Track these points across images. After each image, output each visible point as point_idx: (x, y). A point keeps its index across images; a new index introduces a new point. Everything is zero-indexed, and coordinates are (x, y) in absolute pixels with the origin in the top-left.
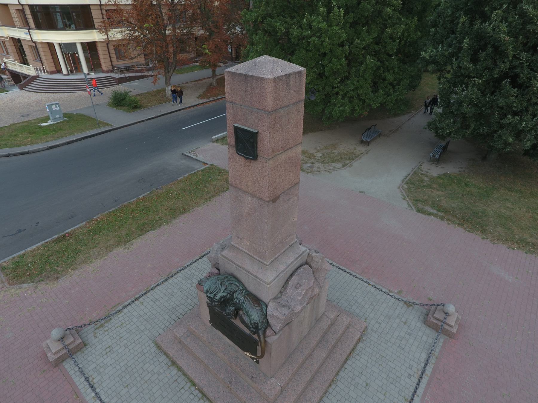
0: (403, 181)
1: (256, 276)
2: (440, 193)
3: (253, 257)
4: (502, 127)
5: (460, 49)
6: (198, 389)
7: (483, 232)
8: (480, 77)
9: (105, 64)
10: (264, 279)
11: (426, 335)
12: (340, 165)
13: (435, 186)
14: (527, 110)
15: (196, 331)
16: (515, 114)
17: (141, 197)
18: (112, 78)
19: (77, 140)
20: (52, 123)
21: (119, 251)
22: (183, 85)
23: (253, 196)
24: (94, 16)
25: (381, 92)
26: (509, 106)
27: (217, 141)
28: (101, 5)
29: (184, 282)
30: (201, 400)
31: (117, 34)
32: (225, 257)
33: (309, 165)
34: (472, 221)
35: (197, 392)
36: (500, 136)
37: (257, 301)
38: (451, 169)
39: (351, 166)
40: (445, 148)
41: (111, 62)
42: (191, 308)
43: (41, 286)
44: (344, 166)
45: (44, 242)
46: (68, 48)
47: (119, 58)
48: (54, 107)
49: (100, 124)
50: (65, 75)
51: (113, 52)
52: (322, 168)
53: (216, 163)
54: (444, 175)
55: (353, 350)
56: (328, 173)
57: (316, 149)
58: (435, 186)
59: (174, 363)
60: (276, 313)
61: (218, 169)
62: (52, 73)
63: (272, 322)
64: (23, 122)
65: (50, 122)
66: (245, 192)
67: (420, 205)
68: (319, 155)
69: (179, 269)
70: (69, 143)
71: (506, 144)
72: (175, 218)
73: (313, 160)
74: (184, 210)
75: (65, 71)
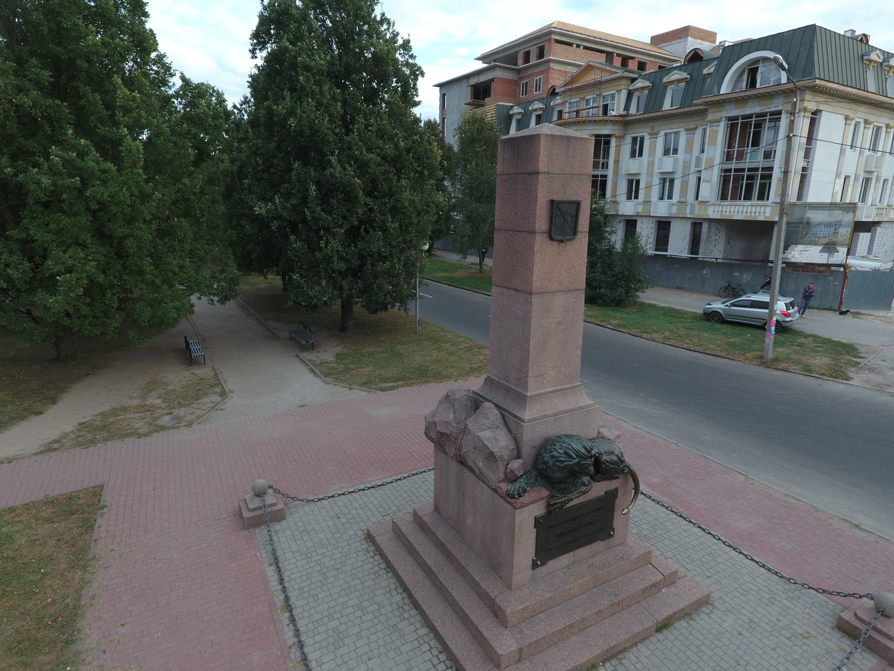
0: (318, 376)
1: (581, 408)
2: (366, 369)
3: (563, 390)
4: (376, 277)
5: (304, 200)
6: (604, 662)
7: (447, 377)
13: (352, 366)
14: (391, 255)
15: (528, 604)
23: (568, 291)
26: (380, 254)
29: (345, 650)
30: (623, 661)
32: (533, 420)
35: (608, 664)
36: (379, 287)
39: (232, 392)
42: (426, 647)
44: (223, 394)
52: (198, 412)
54: (338, 356)
56: (219, 412)
57: (131, 398)
58: (352, 366)
60: (616, 433)
66: (554, 292)
69: (295, 654)
72: (68, 642)
73: (159, 411)
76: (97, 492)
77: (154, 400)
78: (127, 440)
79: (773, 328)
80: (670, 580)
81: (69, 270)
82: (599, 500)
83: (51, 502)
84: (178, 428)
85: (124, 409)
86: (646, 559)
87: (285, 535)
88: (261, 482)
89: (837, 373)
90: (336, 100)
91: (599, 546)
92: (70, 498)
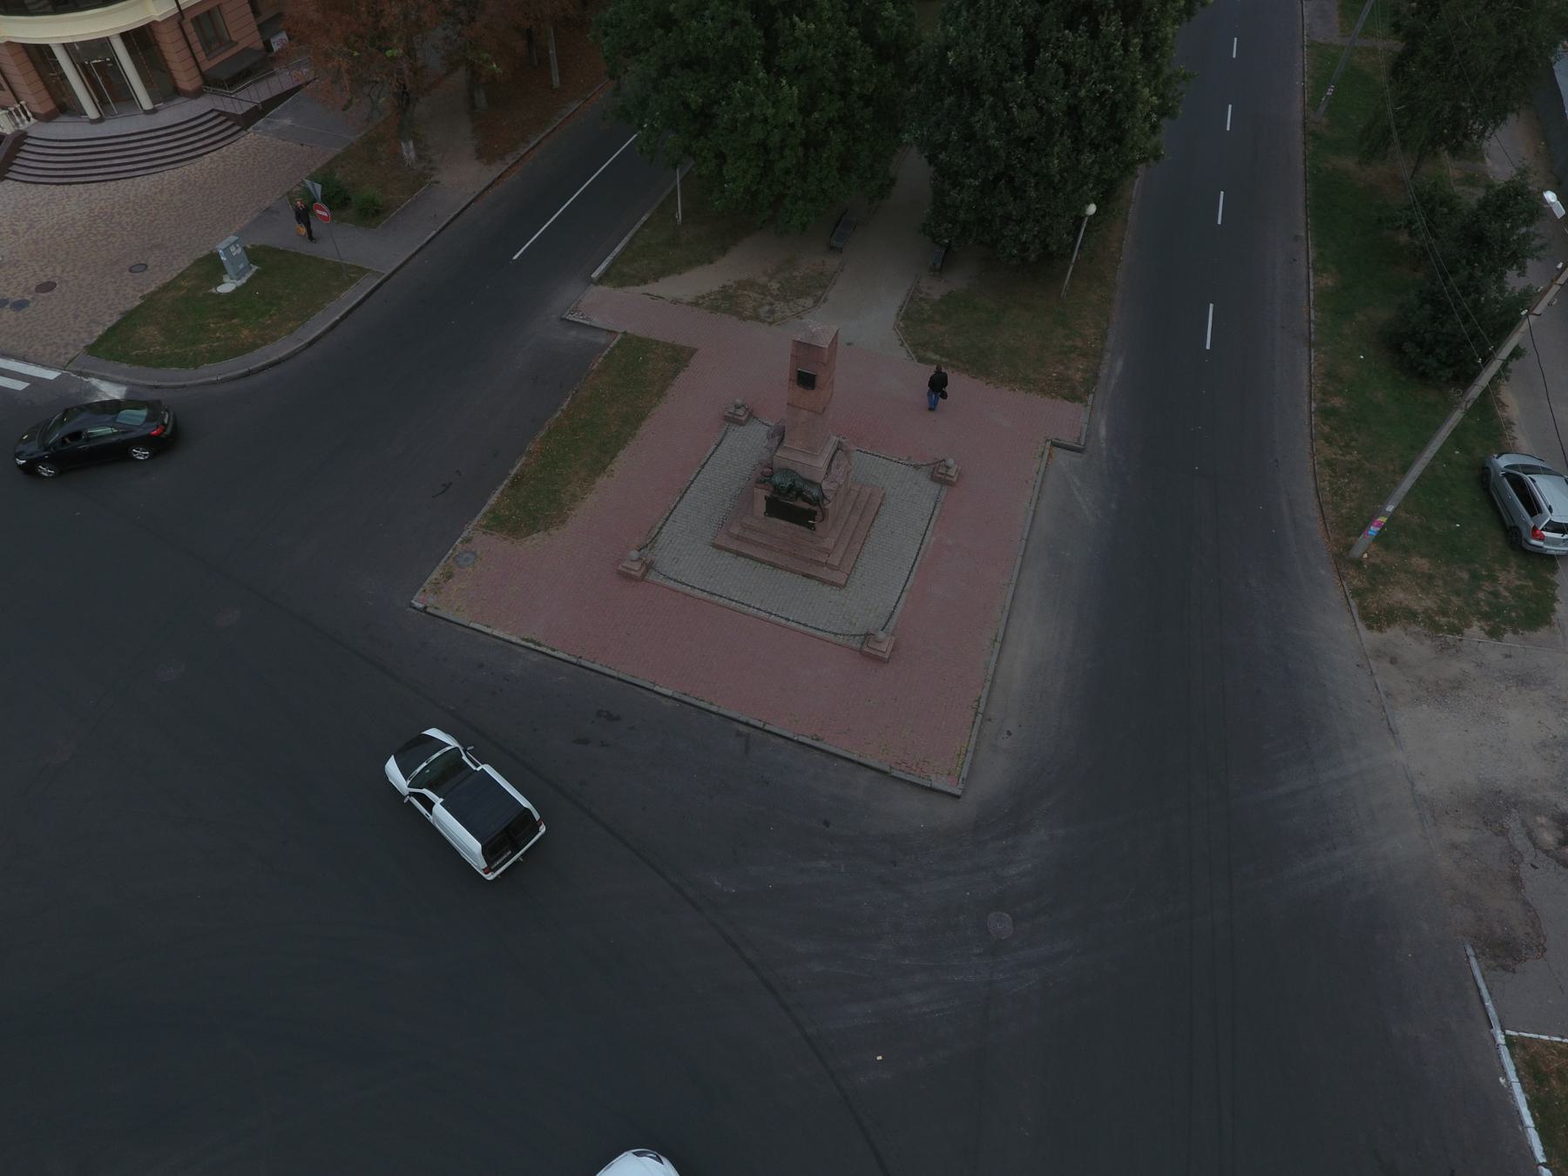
10: (814, 465)
11: (934, 488)
12: (809, 302)
18: (221, 113)
19: (342, 318)
20: (239, 283)
21: (602, 480)
27: (600, 281)
33: (767, 308)
37: (812, 483)
41: (197, 64)
43: (553, 531)
44: (816, 302)
45: (498, 493)
46: (91, 55)
47: (207, 45)
50: (93, 122)
51: (193, 37)
52: (788, 313)
59: (738, 554)
61: (639, 339)
62: (48, 118)
64: (165, 288)
68: (775, 285)
70: (333, 327)
76: (693, 352)
79: (1373, 530)
81: (734, 180)
82: (803, 510)
84: (763, 321)
85: (749, 284)
88: (739, 401)
92: (683, 349)
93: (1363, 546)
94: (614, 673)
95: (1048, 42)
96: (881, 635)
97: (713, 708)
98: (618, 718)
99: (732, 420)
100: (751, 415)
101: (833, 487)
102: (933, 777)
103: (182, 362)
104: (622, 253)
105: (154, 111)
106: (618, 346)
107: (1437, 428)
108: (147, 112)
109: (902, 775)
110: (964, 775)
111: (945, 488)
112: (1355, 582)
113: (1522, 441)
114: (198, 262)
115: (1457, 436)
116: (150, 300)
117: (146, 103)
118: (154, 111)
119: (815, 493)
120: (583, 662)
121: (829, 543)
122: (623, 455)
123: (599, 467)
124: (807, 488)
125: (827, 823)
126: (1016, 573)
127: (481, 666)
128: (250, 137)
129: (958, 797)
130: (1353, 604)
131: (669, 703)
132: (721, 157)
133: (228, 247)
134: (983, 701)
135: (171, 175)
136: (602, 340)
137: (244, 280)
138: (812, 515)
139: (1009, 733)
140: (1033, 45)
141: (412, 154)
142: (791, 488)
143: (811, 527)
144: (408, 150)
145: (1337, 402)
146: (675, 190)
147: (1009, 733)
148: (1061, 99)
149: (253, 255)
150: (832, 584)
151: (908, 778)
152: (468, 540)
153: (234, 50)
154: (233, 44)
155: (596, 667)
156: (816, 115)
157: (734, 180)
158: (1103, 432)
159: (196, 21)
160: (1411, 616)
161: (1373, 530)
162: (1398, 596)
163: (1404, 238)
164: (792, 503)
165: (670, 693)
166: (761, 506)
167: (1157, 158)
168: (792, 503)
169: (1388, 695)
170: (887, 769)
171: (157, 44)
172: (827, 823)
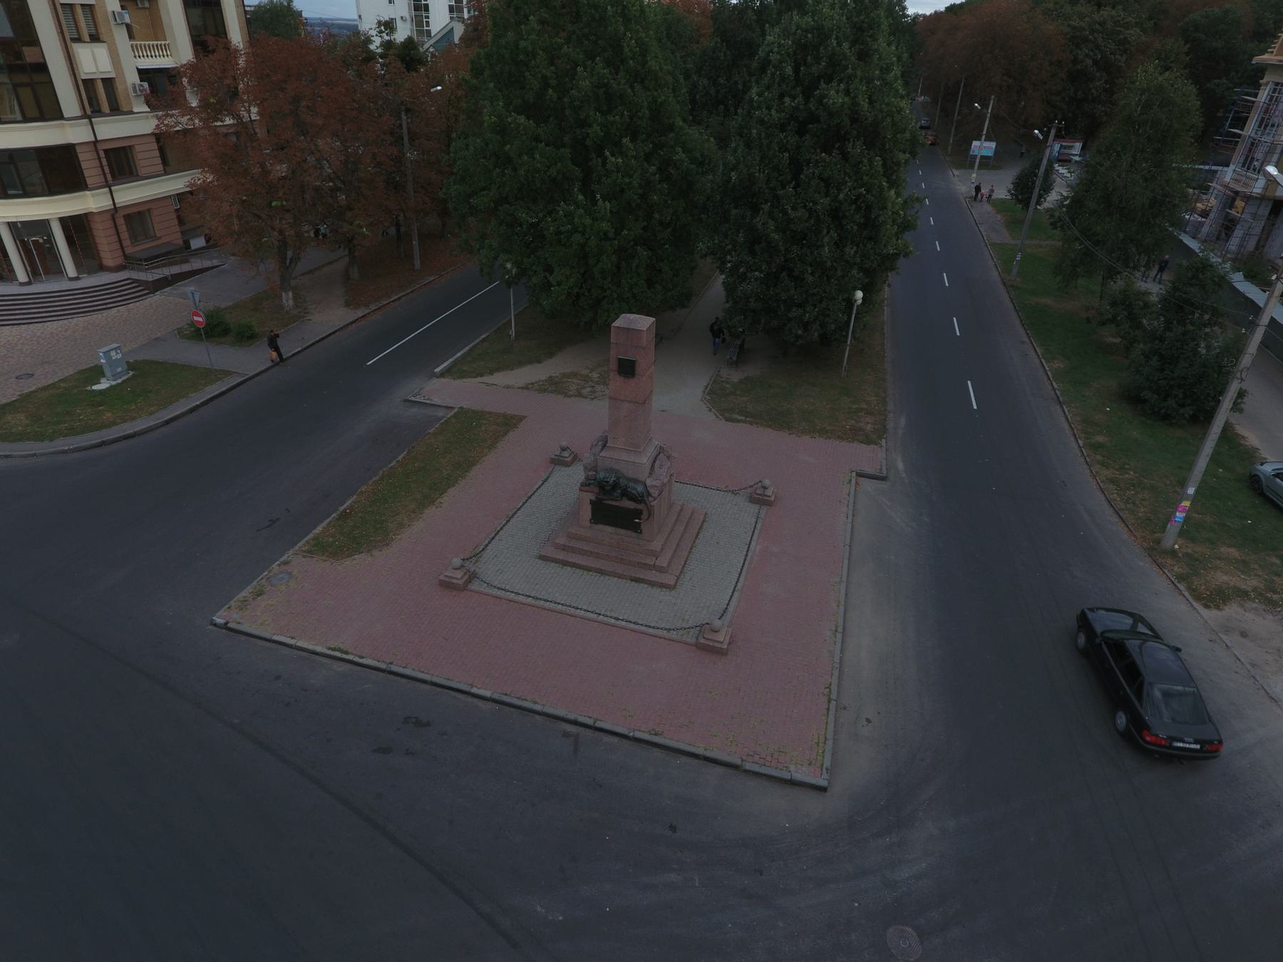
8: (761, 271)
9: (109, 256)
11: (754, 508)
16: (800, 306)
17: (400, 458)
18: (135, 281)
21: (430, 512)
22: (293, 283)
24: (84, 165)
25: (659, 287)
27: (442, 375)
28: (96, 142)
31: (129, 194)
34: (778, 420)
37: (636, 481)
38: (751, 371)
40: (741, 347)
43: (376, 553)
47: (134, 238)
48: (113, 353)
49: (209, 375)
50: (22, 284)
51: (123, 228)
53: (466, 404)
55: (701, 528)
59: (565, 563)
63: (652, 491)
64: (45, 388)
65: (103, 385)
67: (727, 414)
68: (595, 375)
70: (192, 410)
71: (798, 337)
74: (470, 465)
75: (21, 275)
76: (521, 418)
77: (595, 375)
78: (560, 396)
79: (1180, 516)
80: (661, 570)
81: (559, 284)
82: (629, 510)
83: (504, 416)
85: (574, 375)
86: (656, 555)
87: (561, 474)
88: (564, 444)
89: (1216, 598)
90: (787, 150)
91: (634, 534)
92: (513, 417)
93: (1171, 539)
94: (427, 677)
95: (808, 162)
96: (717, 623)
97: (538, 708)
98: (428, 724)
99: (557, 462)
100: (575, 458)
101: (657, 483)
102: (792, 768)
103: (39, 437)
104: (464, 357)
105: (77, 279)
106: (454, 416)
107: (1197, 452)
108: (71, 279)
109: (756, 768)
110: (827, 763)
111: (764, 509)
112: (1176, 569)
113: (1270, 459)
114: (80, 372)
115: (1215, 459)
116: (26, 398)
117: (71, 270)
118: (77, 279)
119: (640, 488)
120: (394, 668)
121: (656, 545)
122: (451, 491)
123: (428, 501)
124: (631, 484)
125: (673, 828)
126: (845, 569)
127: (278, 678)
128: (158, 297)
129: (823, 789)
130: (1181, 587)
131: (489, 705)
132: (549, 269)
133: (111, 354)
134: (834, 688)
135: (80, 321)
136: (440, 413)
137: (119, 381)
138: (638, 513)
139: (868, 721)
140: (797, 166)
141: (291, 303)
142: (615, 485)
143: (636, 528)
144: (288, 299)
145: (1100, 439)
146: (510, 321)
147: (868, 721)
148: (825, 201)
149: (131, 366)
150: (662, 586)
151: (763, 770)
152: (286, 563)
153: (155, 243)
154: (155, 238)
155: (408, 672)
156: (625, 232)
157: (559, 284)
158: (901, 466)
159: (128, 218)
160: (1242, 595)
161: (1180, 516)
162: (1222, 578)
163: (1110, 336)
164: (617, 505)
165: (488, 694)
166: (587, 512)
167: (906, 255)
168: (617, 505)
169: (1253, 665)
170: (738, 762)
171: (93, 236)
172: (673, 828)
